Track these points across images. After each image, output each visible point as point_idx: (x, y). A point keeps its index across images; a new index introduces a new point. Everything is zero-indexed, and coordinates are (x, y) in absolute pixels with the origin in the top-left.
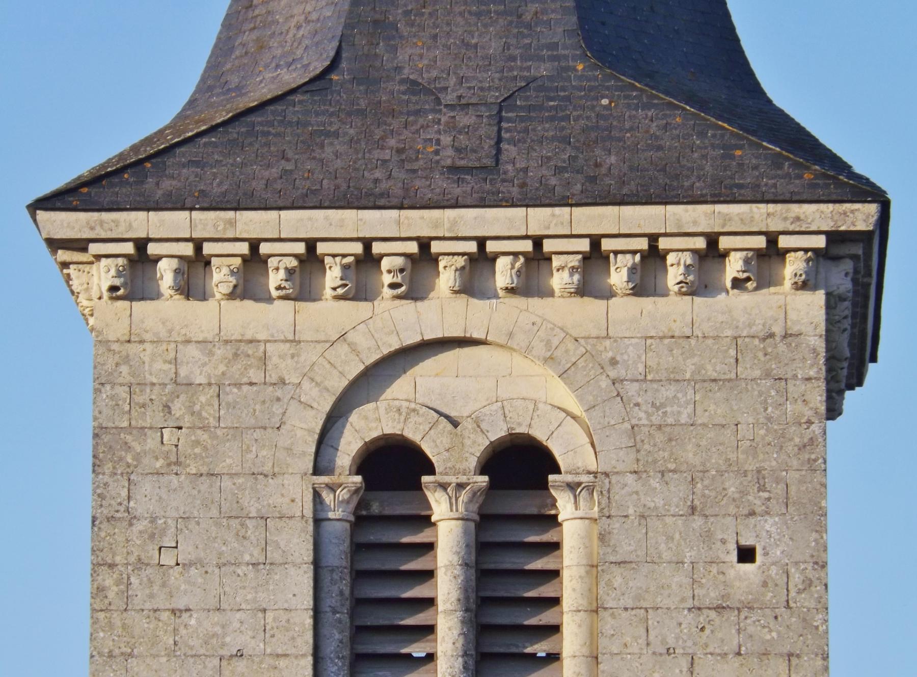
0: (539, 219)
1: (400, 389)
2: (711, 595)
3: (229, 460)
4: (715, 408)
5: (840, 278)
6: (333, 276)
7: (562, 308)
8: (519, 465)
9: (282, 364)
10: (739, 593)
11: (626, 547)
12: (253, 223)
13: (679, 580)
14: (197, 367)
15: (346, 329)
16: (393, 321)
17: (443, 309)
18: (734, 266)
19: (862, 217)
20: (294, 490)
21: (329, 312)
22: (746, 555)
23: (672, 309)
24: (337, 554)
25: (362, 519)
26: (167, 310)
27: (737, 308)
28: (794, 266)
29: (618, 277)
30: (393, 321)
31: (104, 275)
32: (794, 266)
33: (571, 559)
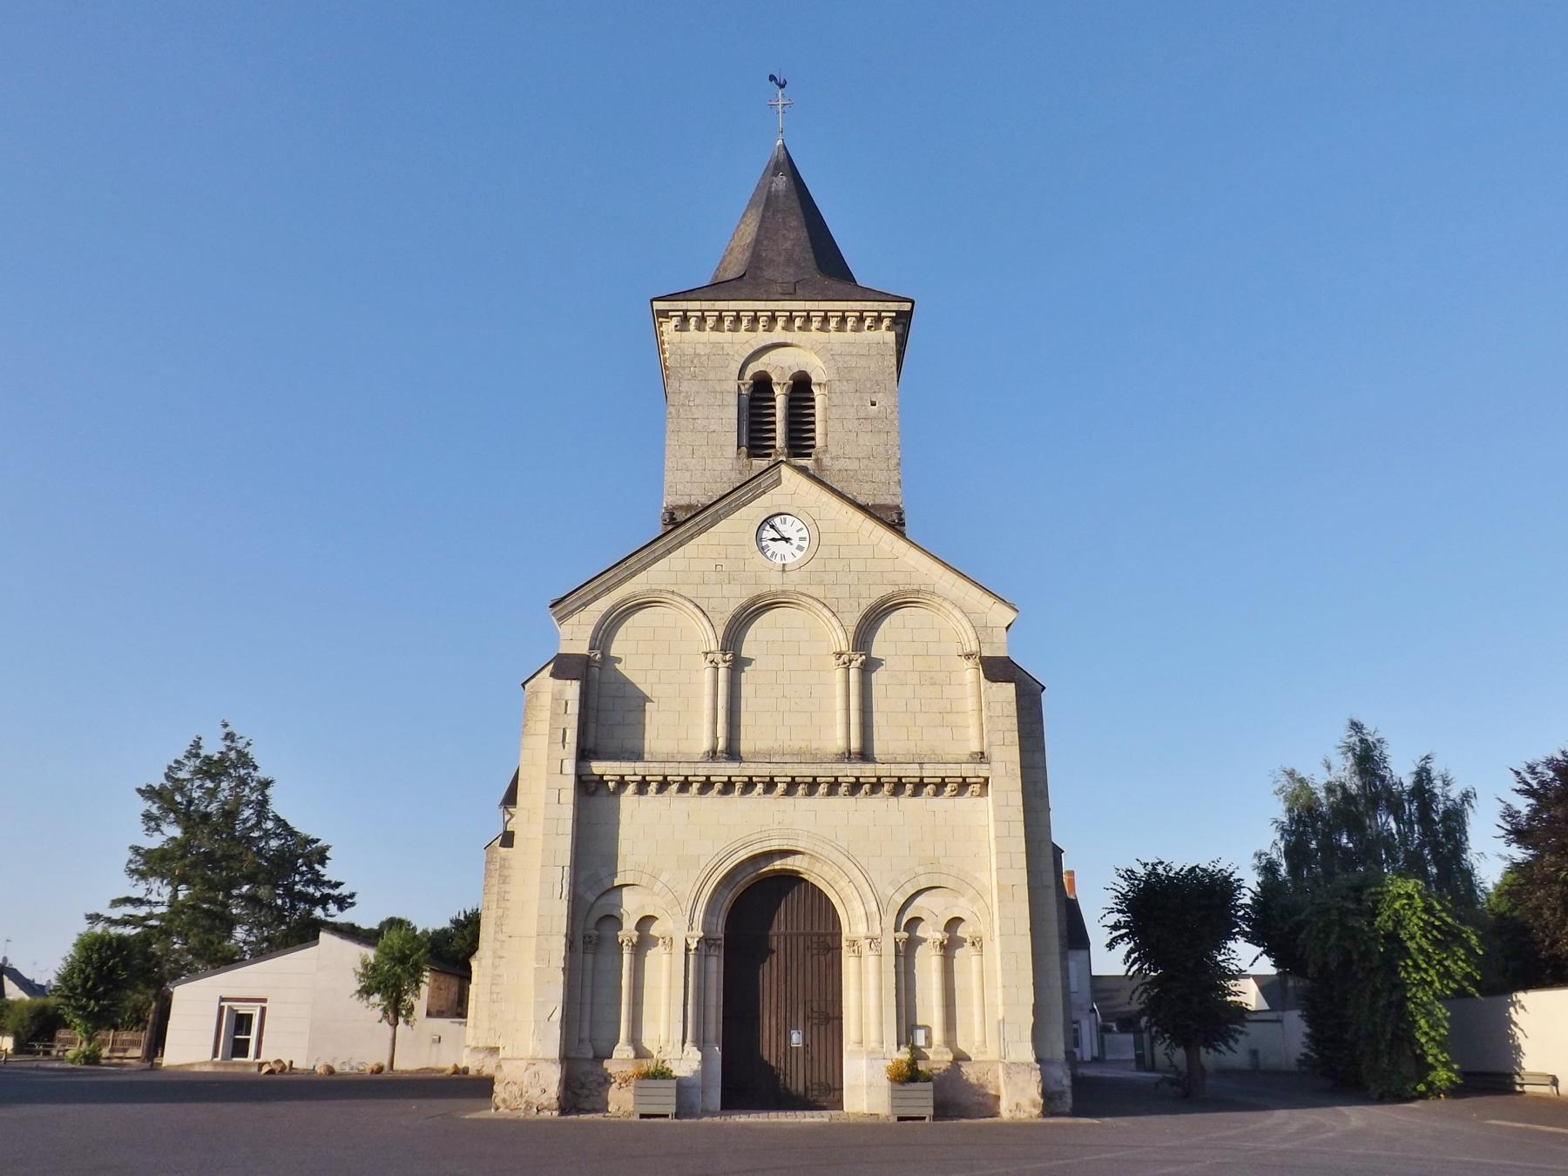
0: (809, 305)
1: (765, 358)
2: (862, 415)
3: (712, 376)
4: (862, 363)
5: (899, 328)
6: (745, 322)
7: (814, 335)
8: (801, 385)
9: (728, 349)
10: (871, 414)
11: (836, 401)
12: (720, 305)
13: (853, 410)
14: (701, 350)
15: (745, 340)
16: (762, 338)
17: (779, 334)
18: (868, 322)
19: (906, 306)
20: (732, 385)
21: (742, 335)
22: (873, 404)
23: (848, 335)
24: (745, 403)
25: (752, 399)
26: (692, 334)
27: (867, 335)
28: (886, 322)
29: (833, 323)
30: (762, 338)
31: (675, 321)
32: (886, 322)
33: (819, 411)
